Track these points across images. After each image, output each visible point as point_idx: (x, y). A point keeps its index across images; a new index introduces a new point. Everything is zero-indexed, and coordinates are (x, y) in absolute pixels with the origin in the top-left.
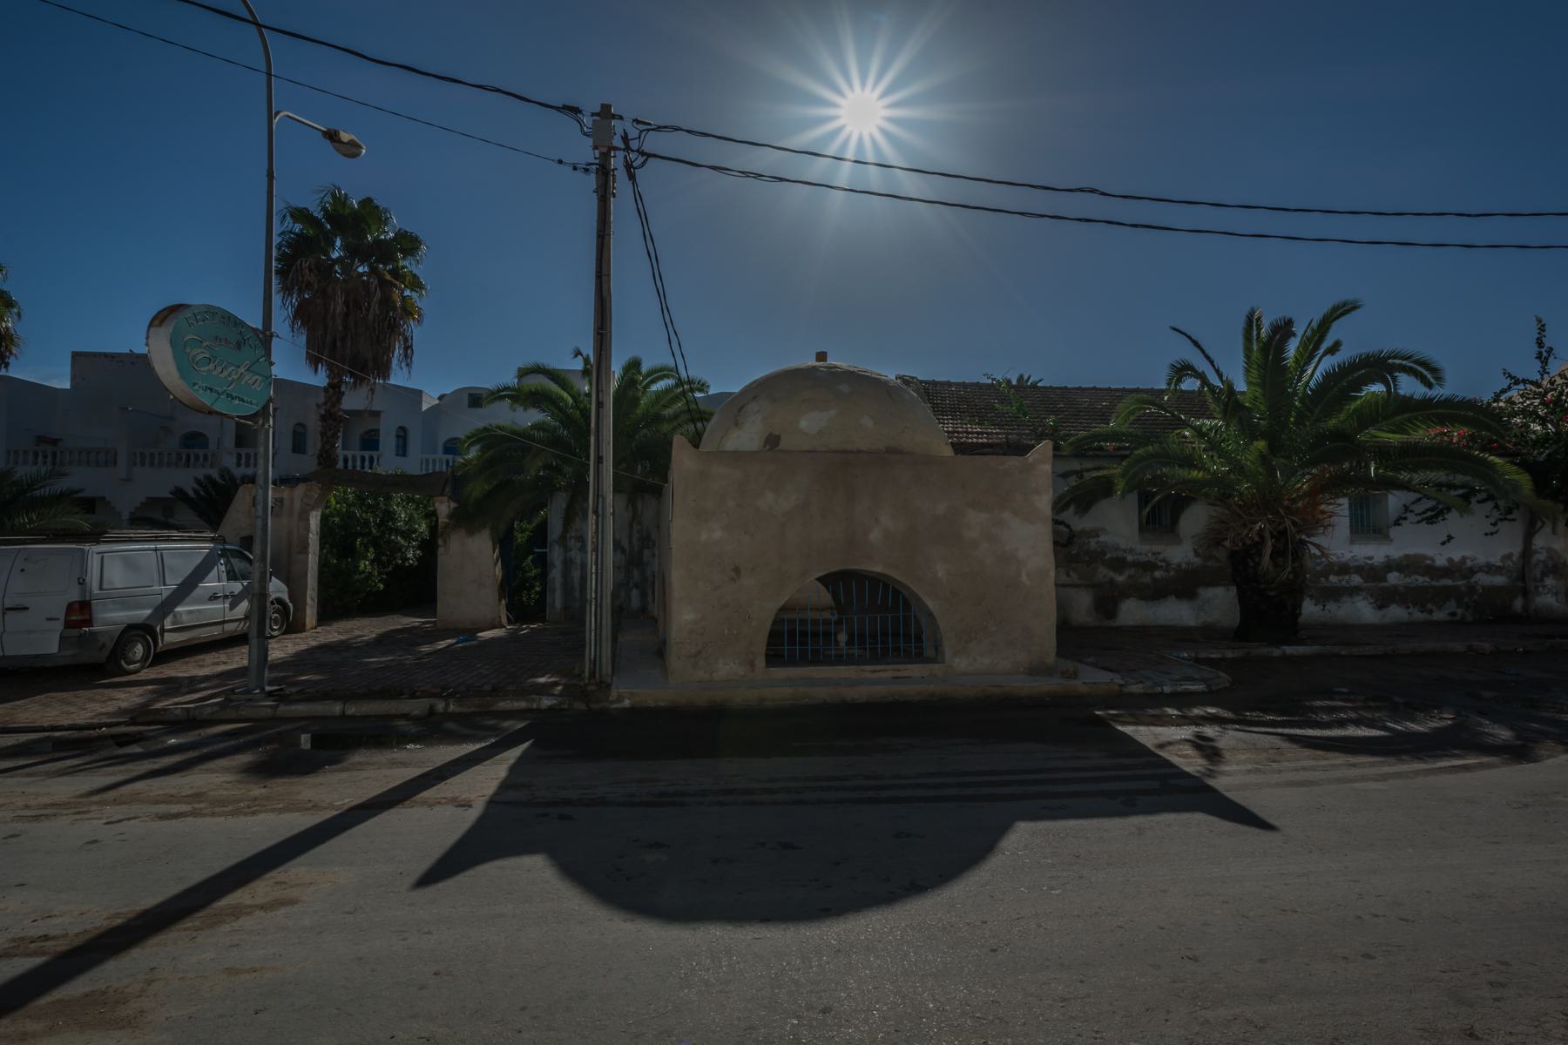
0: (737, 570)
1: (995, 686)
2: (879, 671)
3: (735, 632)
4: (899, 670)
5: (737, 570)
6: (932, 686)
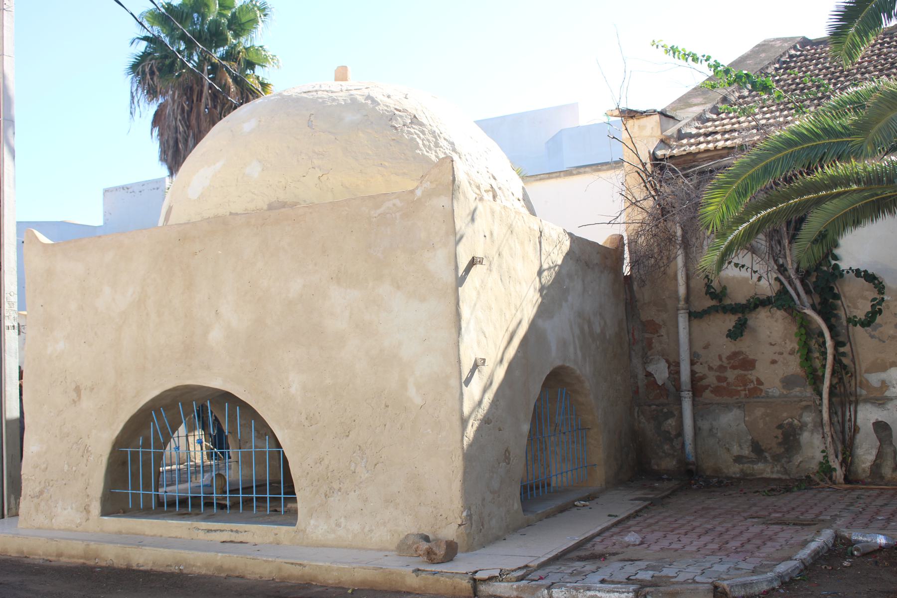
0: (78, 390)
1: (296, 564)
2: (215, 531)
3: (74, 468)
4: (237, 531)
5: (78, 390)
6: (220, 554)
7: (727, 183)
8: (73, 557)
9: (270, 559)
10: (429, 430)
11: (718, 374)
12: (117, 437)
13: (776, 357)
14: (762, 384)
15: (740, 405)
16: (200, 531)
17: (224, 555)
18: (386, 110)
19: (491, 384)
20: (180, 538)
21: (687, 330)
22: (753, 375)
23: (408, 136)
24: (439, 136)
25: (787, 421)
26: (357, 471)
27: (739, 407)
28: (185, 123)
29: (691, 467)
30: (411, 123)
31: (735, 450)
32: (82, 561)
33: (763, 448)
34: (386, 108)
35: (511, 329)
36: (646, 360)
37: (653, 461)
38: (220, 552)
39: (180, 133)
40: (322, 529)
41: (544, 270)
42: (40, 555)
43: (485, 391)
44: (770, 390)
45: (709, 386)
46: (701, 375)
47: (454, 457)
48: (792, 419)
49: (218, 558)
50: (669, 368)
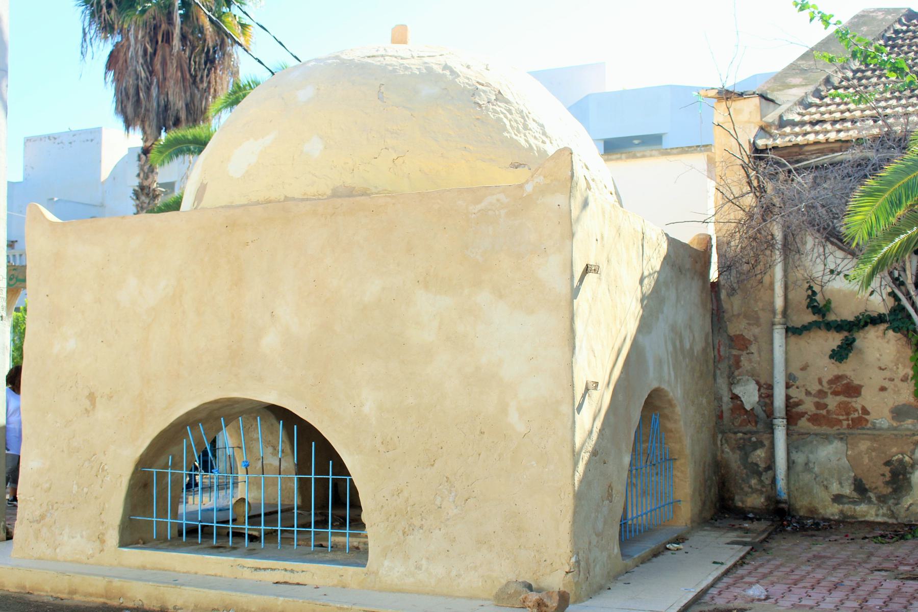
0: (92, 397)
2: (265, 569)
3: (85, 490)
4: (292, 571)
5: (92, 397)
6: (281, 599)
7: (879, 191)
8: (91, 595)
9: (345, 606)
10: (533, 463)
11: (817, 400)
12: (142, 456)
13: (886, 384)
14: (868, 413)
15: (841, 437)
16: (245, 569)
17: (286, 599)
18: (467, 84)
19: (599, 411)
20: (220, 576)
21: (783, 349)
22: (857, 403)
23: (494, 116)
24: (527, 116)
25: (896, 457)
26: (443, 507)
27: (841, 439)
28: (148, 68)
29: (783, 505)
30: (496, 100)
31: (835, 488)
32: (102, 600)
33: (867, 487)
34: (467, 81)
35: (616, 348)
36: (732, 381)
37: (737, 498)
38: (280, 596)
39: (141, 80)
40: (398, 572)
41: (645, 278)
42: (47, 592)
43: (594, 420)
44: (877, 421)
45: (806, 413)
46: (796, 400)
47: (563, 493)
48: (902, 455)
49: (279, 603)
50: (759, 390)
